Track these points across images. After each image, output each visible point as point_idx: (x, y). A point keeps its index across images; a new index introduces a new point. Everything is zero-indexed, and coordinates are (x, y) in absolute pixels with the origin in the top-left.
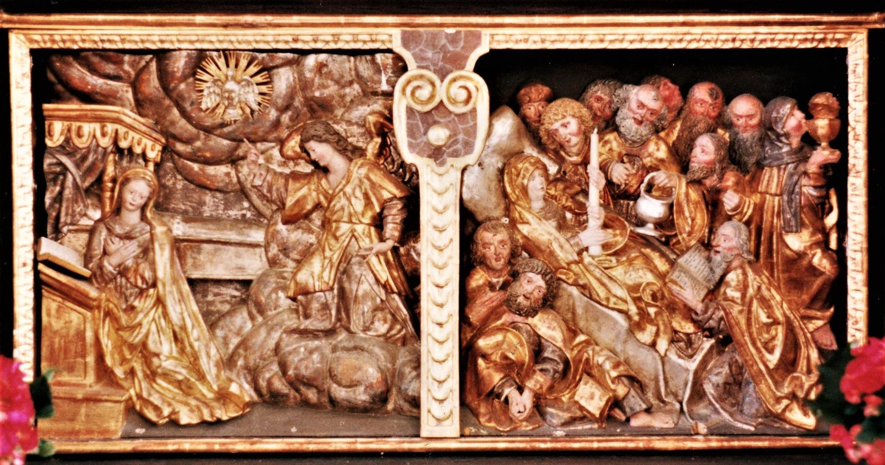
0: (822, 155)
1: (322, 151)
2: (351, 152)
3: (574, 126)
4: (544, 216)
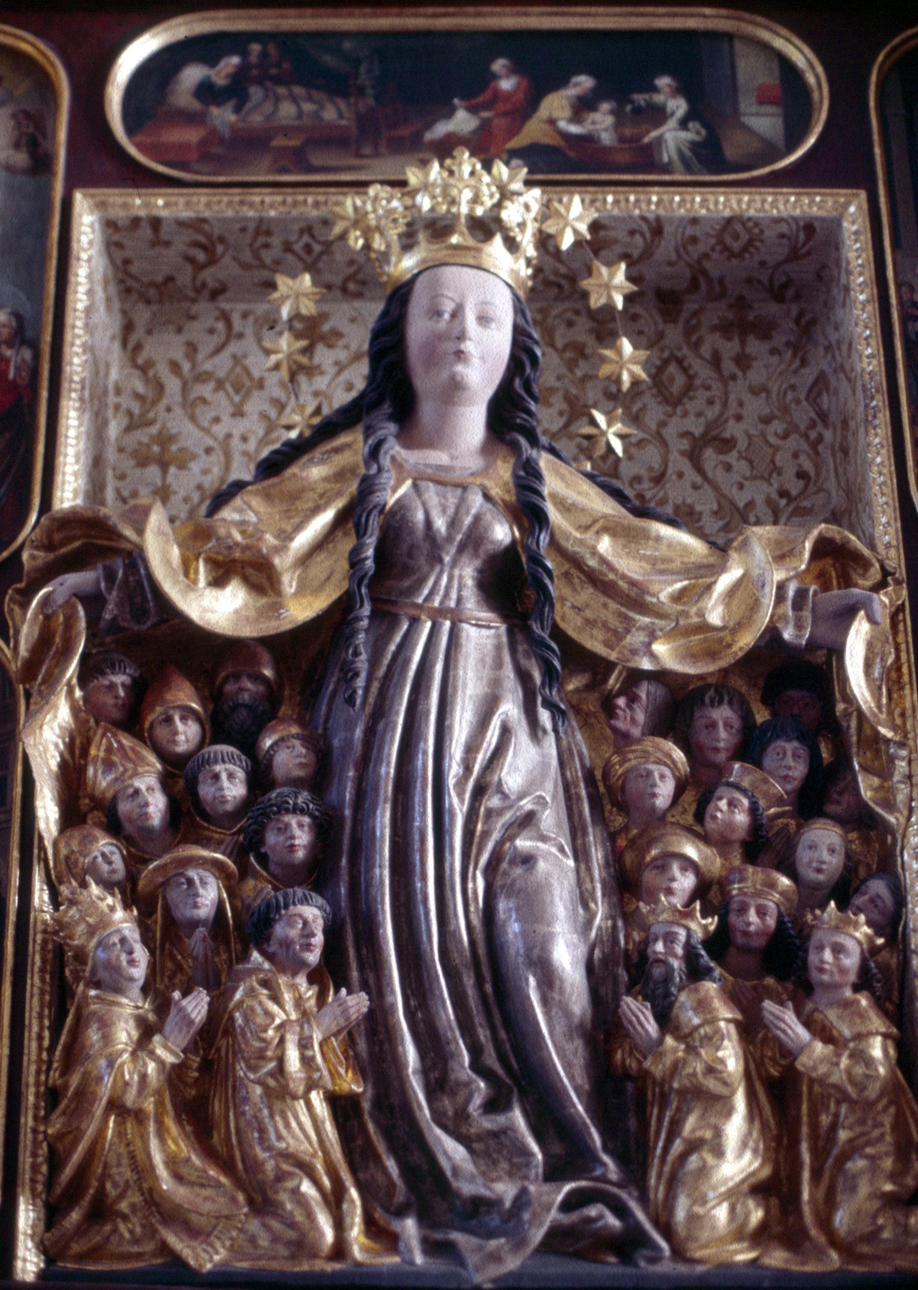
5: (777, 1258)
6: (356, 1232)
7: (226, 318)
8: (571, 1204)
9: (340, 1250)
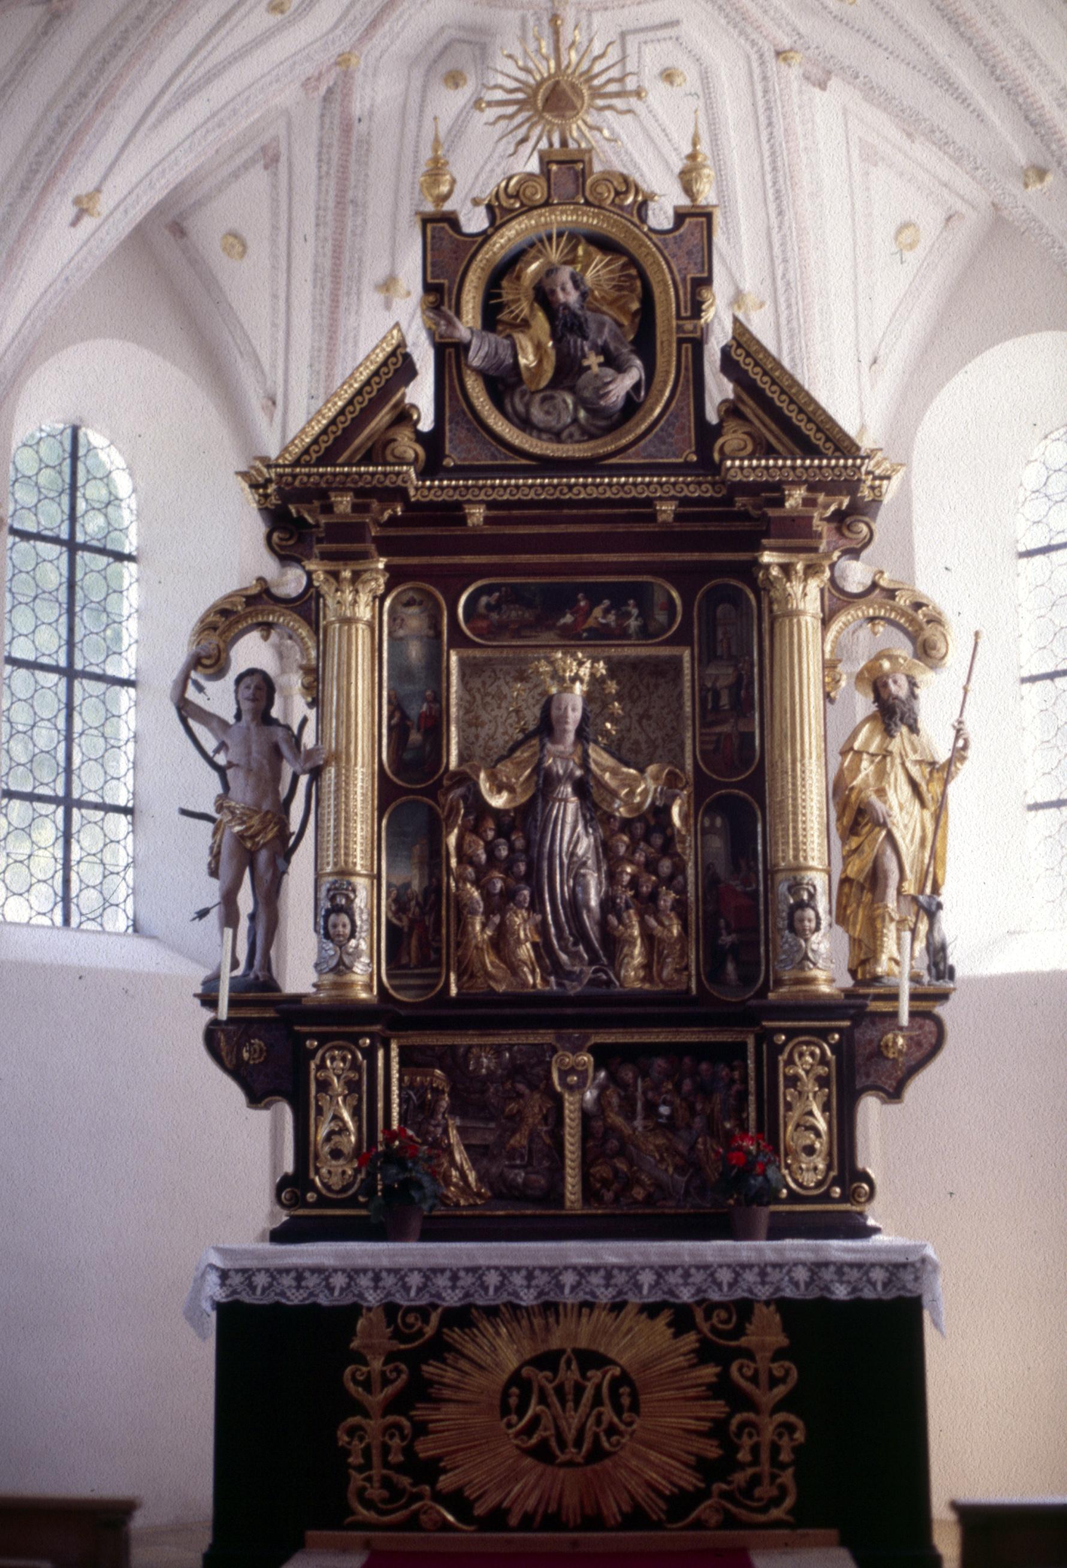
0: (736, 1087)
1: (521, 1087)
2: (533, 1087)
3: (630, 1075)
4: (618, 1114)
5: (647, 986)
6: (538, 981)
7: (494, 671)
8: (595, 972)
9: (534, 985)
